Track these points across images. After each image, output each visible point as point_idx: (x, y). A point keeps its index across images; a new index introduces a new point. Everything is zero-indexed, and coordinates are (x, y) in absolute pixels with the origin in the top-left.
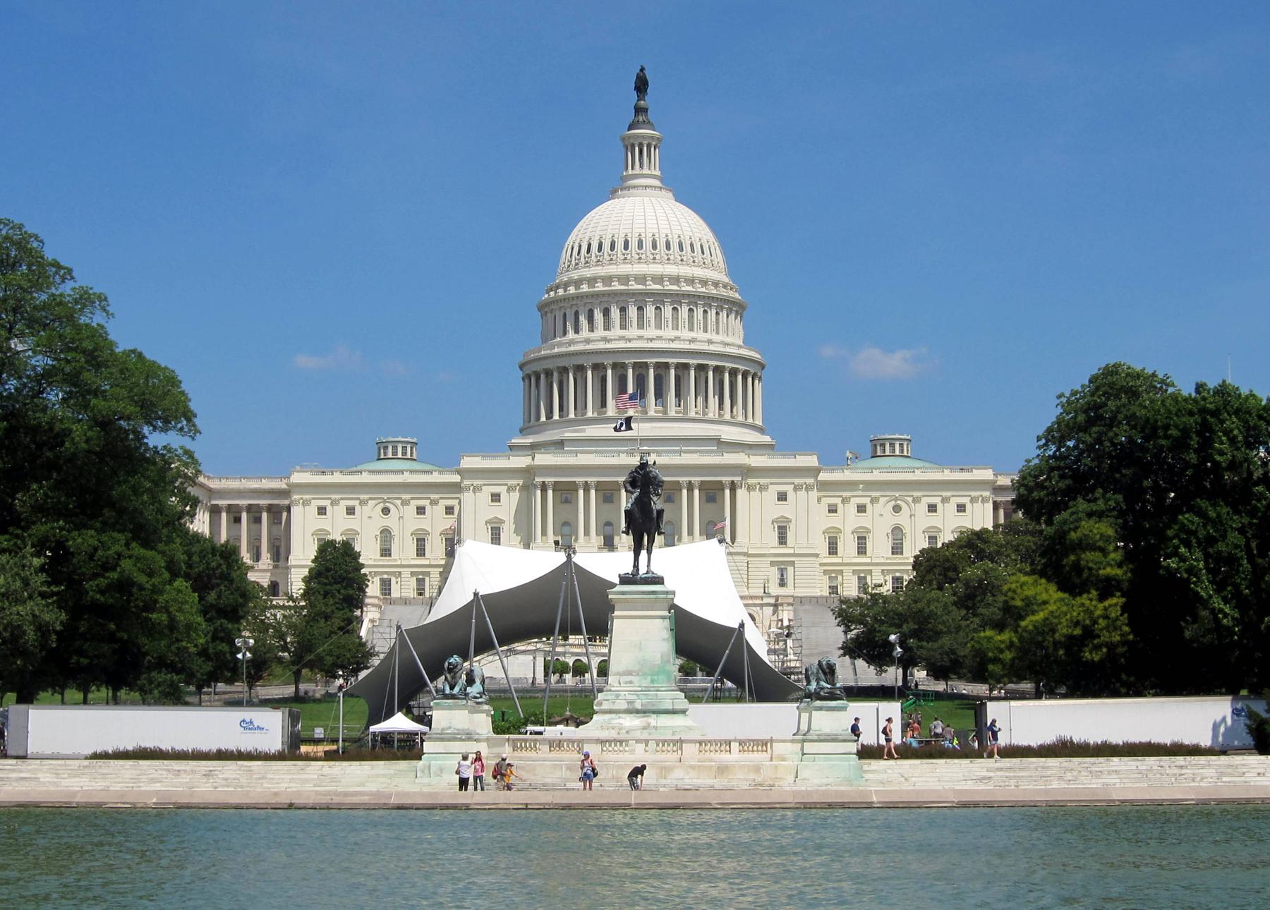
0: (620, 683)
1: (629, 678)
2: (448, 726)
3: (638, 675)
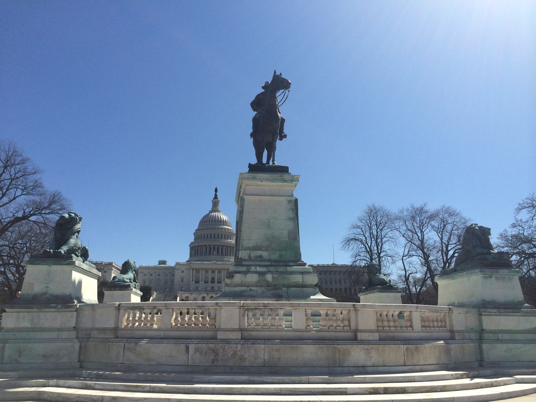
1: (259, 253)
2: (43, 291)
3: (267, 250)
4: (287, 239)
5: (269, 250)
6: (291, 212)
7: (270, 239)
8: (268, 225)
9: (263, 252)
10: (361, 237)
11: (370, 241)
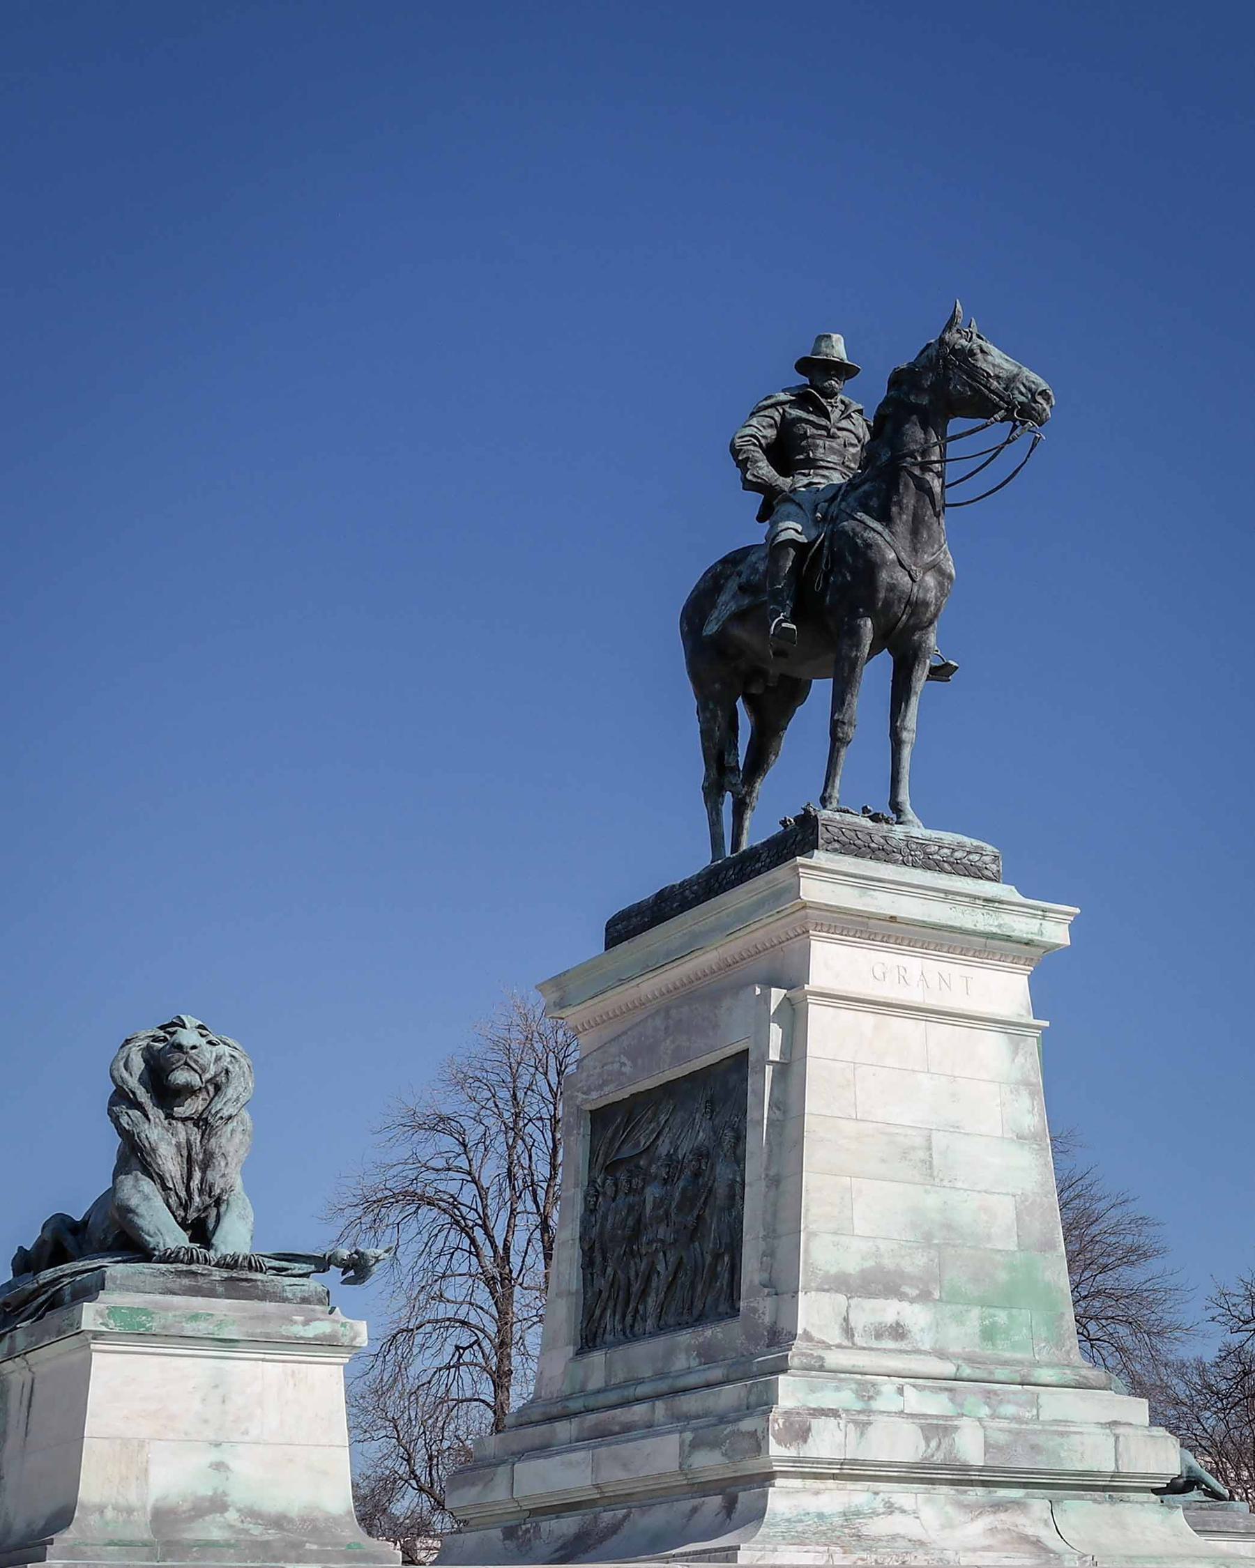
0: (848, 1331)
1: (890, 1310)
3: (924, 1297)
4: (1012, 1246)
5: (936, 1295)
6: (1025, 1101)
7: (936, 1241)
8: (923, 1161)
9: (905, 1304)
10: (453, 1187)
11: (504, 1216)
